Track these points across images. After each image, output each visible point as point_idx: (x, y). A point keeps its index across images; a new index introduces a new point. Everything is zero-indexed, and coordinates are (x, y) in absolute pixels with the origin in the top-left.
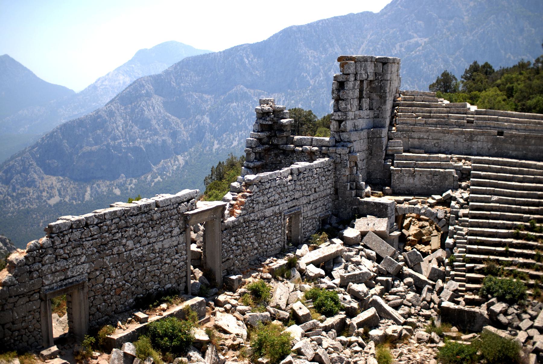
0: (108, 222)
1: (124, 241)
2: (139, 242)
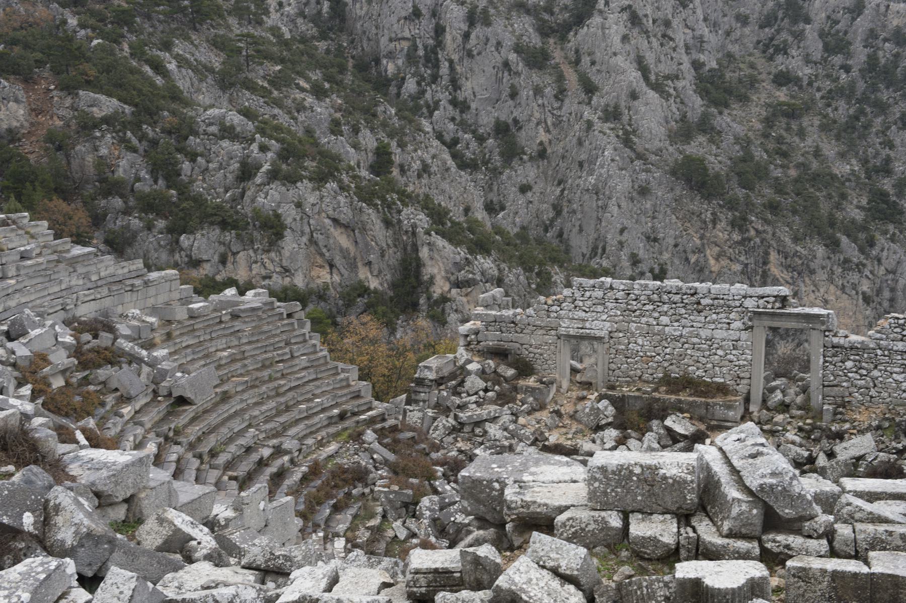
0: (636, 292)
1: (656, 315)
2: (677, 321)
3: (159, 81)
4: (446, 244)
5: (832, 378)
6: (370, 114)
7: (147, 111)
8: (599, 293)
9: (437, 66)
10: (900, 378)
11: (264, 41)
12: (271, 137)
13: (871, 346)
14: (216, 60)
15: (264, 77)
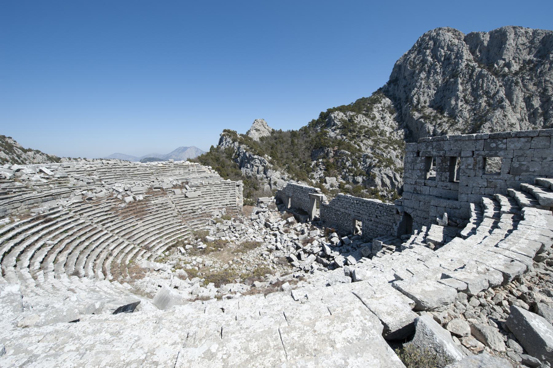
3: (358, 148)
7: (353, 153)
11: (385, 139)
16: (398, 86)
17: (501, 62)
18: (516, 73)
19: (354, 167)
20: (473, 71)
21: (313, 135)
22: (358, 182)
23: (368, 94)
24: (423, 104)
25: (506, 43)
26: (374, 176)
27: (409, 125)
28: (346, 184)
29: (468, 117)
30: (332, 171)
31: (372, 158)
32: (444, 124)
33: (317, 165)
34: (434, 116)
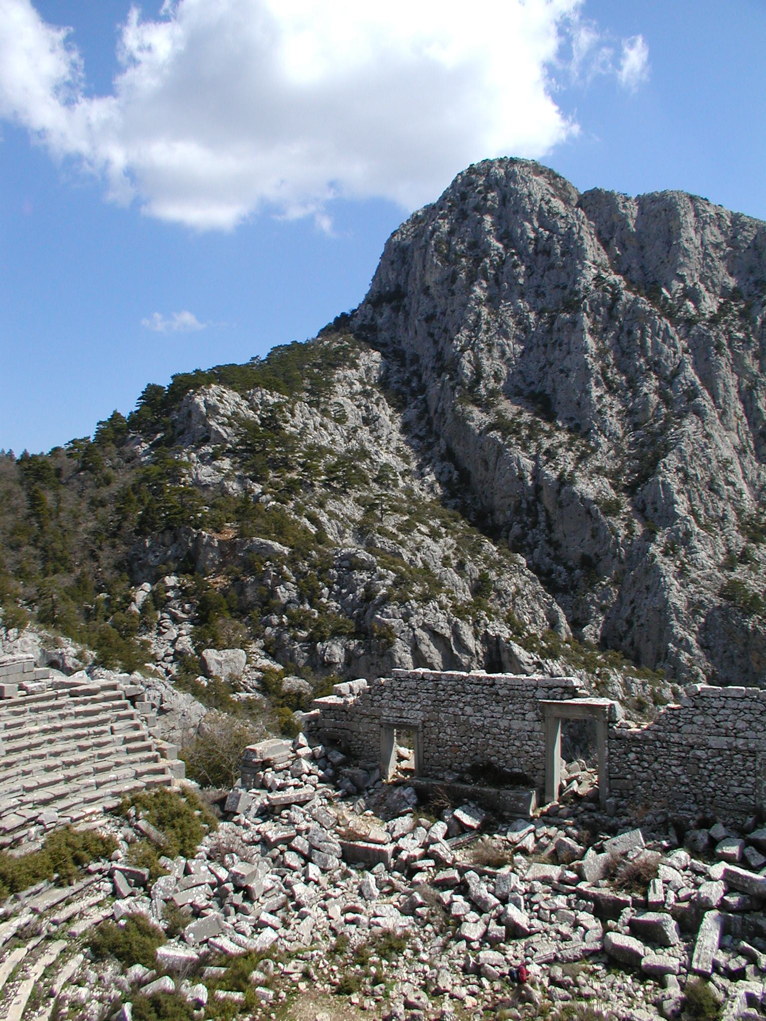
0: (443, 682)
1: (461, 705)
3: (313, 530)
4: (522, 651)
5: (617, 770)
6: (476, 549)
7: (299, 552)
8: (412, 684)
9: (537, 515)
10: (677, 770)
11: (397, 499)
12: (388, 569)
13: (651, 737)
14: (358, 515)
15: (394, 526)
16: (407, 315)
17: (677, 285)
18: (714, 321)
19: (307, 607)
20: (616, 297)
21: (124, 478)
22: (331, 664)
23: (306, 331)
24: (492, 384)
25: (680, 236)
26: (387, 636)
27: (458, 449)
28: (287, 673)
29: (620, 433)
30: (226, 625)
31: (370, 568)
32: (561, 451)
33: (158, 601)
34: (531, 427)
